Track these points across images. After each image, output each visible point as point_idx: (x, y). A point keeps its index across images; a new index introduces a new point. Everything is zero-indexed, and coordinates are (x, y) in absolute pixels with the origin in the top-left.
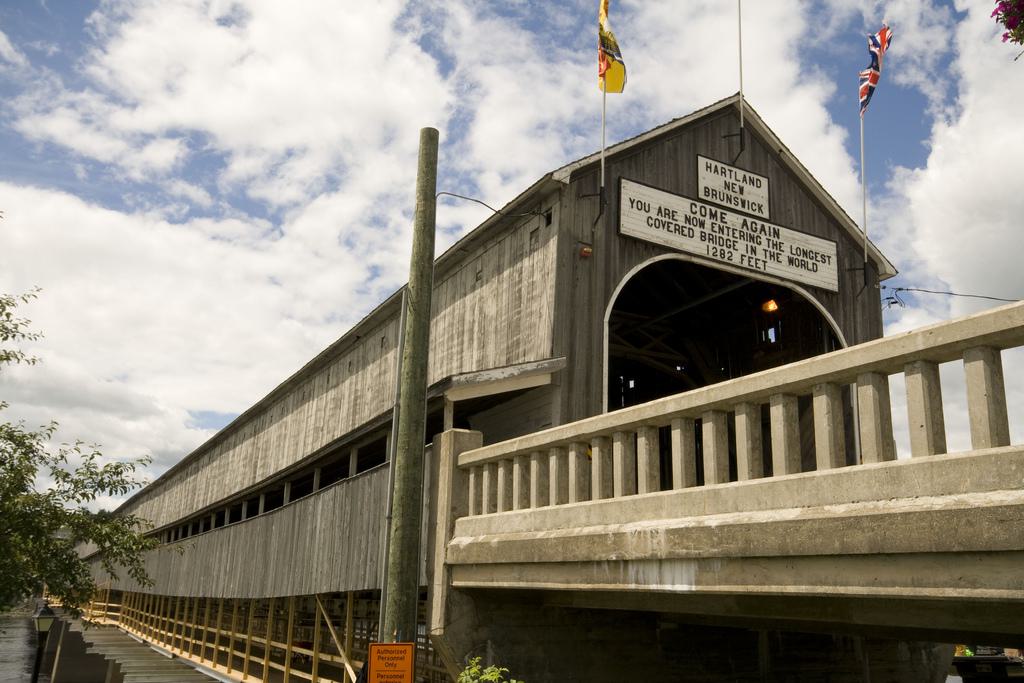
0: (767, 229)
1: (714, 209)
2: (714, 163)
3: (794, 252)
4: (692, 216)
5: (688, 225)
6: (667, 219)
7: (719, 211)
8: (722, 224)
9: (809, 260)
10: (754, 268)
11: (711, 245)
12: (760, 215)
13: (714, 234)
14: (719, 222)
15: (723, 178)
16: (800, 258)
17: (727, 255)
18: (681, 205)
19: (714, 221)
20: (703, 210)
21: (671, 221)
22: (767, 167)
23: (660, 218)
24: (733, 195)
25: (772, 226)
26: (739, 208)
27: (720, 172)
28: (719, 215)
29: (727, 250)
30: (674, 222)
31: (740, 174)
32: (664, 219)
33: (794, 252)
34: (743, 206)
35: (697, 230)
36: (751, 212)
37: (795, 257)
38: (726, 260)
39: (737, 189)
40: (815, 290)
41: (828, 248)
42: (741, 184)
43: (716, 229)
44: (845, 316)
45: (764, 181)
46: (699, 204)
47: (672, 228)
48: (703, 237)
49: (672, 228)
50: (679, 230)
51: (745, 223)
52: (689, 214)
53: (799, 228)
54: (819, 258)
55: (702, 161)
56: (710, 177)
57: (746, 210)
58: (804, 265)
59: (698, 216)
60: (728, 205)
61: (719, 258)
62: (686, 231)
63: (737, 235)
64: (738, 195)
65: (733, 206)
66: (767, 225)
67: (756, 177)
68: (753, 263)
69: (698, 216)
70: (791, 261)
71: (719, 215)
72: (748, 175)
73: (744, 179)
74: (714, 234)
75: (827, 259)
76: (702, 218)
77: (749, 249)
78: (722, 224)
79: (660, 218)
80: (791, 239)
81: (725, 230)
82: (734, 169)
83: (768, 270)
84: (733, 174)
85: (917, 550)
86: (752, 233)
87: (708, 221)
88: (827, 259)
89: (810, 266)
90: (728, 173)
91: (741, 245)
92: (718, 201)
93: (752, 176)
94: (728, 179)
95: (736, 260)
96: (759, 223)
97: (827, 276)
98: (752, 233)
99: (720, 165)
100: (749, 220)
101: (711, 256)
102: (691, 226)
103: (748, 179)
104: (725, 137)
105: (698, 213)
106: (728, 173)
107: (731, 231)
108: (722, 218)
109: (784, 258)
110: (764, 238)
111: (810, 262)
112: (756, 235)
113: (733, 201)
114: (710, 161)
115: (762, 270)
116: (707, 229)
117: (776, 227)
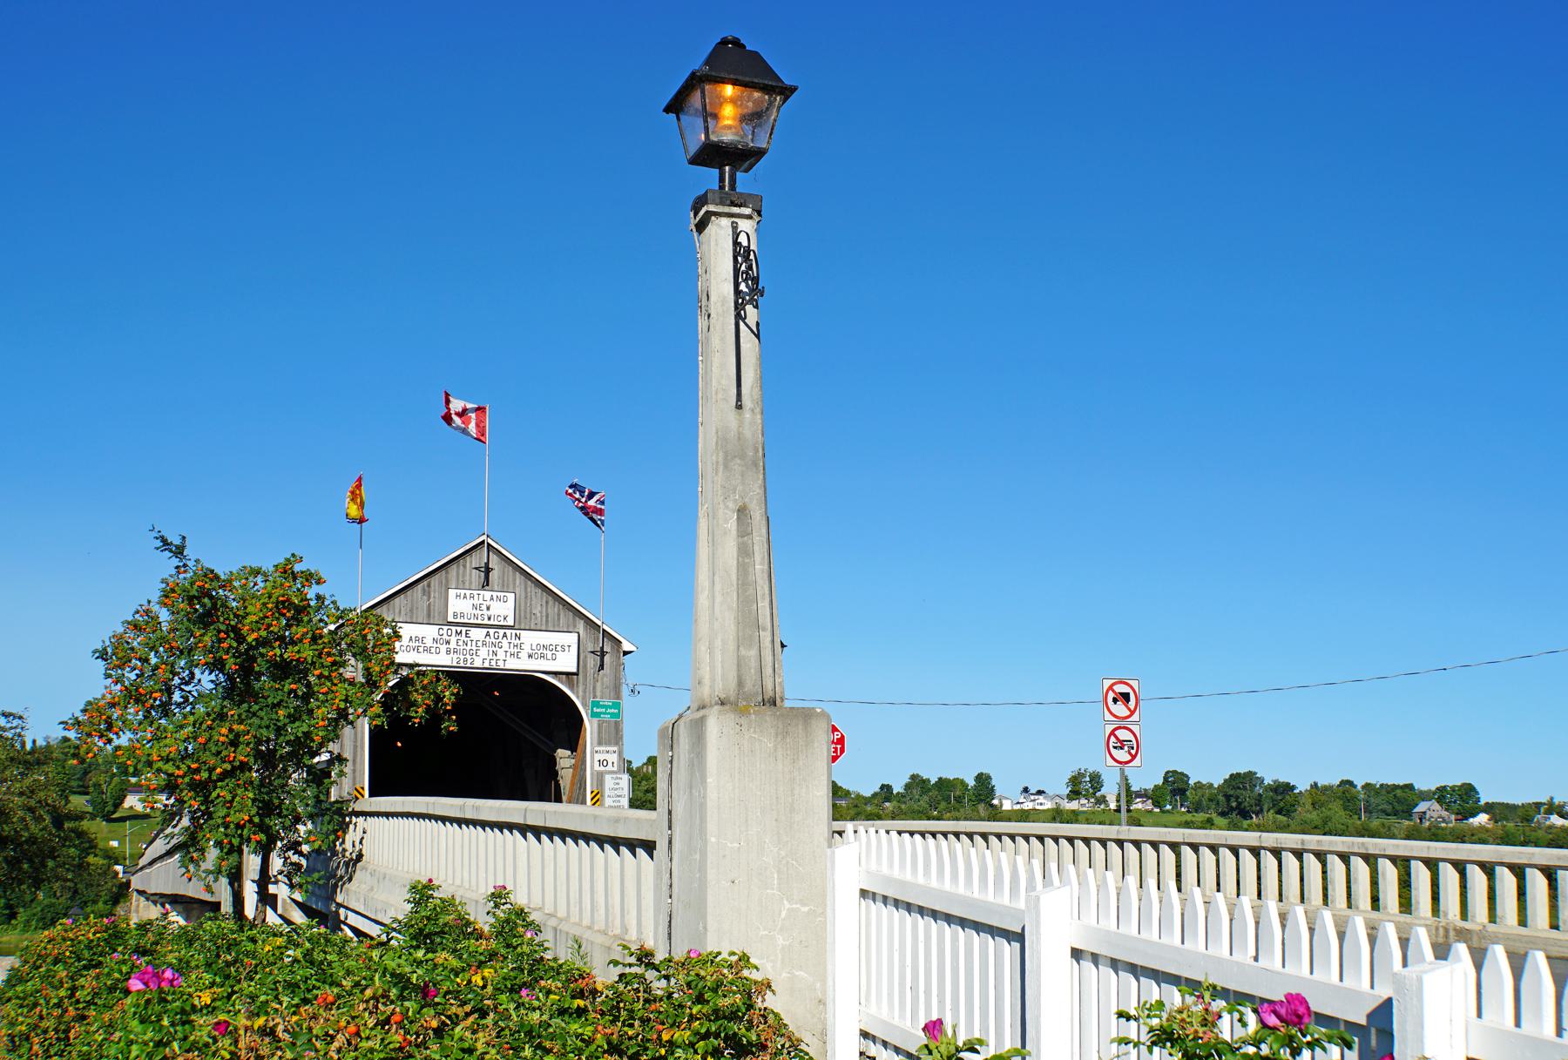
0: (509, 635)
1: (459, 629)
2: (463, 592)
3: (534, 647)
4: (439, 637)
5: (435, 645)
6: (417, 644)
7: (464, 629)
8: (466, 639)
9: (548, 652)
10: (495, 667)
11: (455, 656)
12: (505, 624)
13: (458, 648)
14: (463, 638)
15: (472, 601)
16: (539, 652)
17: (469, 661)
18: (430, 632)
19: (459, 638)
20: (449, 631)
21: (420, 644)
22: (514, 584)
23: (411, 644)
24: (481, 613)
25: (514, 632)
26: (486, 622)
27: (468, 597)
28: (464, 633)
29: (468, 657)
30: (423, 645)
31: (487, 594)
32: (414, 645)
33: (534, 647)
34: (489, 619)
35: (443, 648)
36: (496, 623)
37: (536, 651)
38: (468, 665)
39: (484, 607)
40: (555, 674)
41: (571, 639)
42: (488, 603)
43: (461, 643)
44: (585, 692)
45: (511, 596)
46: (446, 628)
47: (421, 649)
48: (448, 652)
49: (421, 649)
50: (428, 650)
51: (488, 634)
52: (436, 636)
53: (544, 628)
54: (559, 648)
55: (452, 593)
56: (459, 603)
57: (491, 622)
58: (542, 656)
59: (445, 637)
60: (476, 622)
61: (462, 665)
62: (433, 650)
63: (480, 644)
64: (485, 612)
65: (479, 622)
66: (508, 632)
67: (503, 594)
68: (493, 663)
69: (445, 637)
70: (530, 656)
71: (464, 633)
72: (495, 594)
73: (492, 599)
74: (458, 648)
75: (567, 648)
76: (448, 638)
77: (491, 653)
78: (466, 639)
79: (411, 644)
80: (530, 638)
81: (469, 643)
82: (482, 592)
83: (507, 667)
84: (481, 597)
85: (517, 860)
86: (494, 641)
87: (453, 639)
88: (567, 648)
89: (549, 656)
90: (476, 597)
91: (483, 652)
92: (466, 621)
93: (499, 594)
94: (476, 602)
95: (478, 663)
96: (501, 632)
97: (568, 663)
98: (494, 641)
99: (468, 592)
100: (492, 631)
101: (455, 664)
102: (438, 645)
103: (495, 598)
104: (476, 568)
105: (445, 634)
106: (476, 597)
107: (474, 643)
108: (466, 634)
109: (524, 655)
110: (505, 642)
111: (549, 654)
112: (498, 641)
113: (479, 618)
114: (459, 591)
115: (502, 667)
116: (453, 645)
117: (518, 632)
